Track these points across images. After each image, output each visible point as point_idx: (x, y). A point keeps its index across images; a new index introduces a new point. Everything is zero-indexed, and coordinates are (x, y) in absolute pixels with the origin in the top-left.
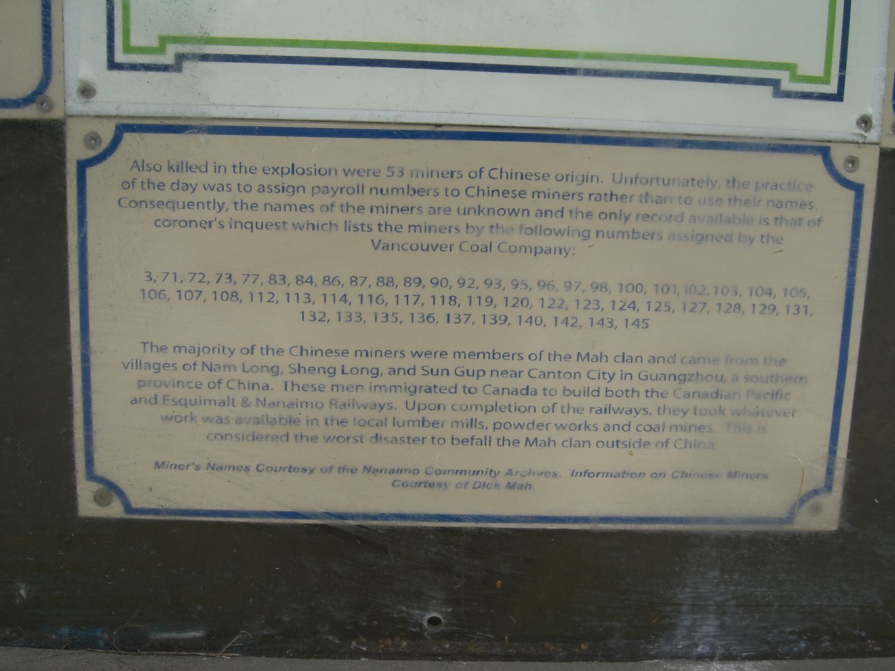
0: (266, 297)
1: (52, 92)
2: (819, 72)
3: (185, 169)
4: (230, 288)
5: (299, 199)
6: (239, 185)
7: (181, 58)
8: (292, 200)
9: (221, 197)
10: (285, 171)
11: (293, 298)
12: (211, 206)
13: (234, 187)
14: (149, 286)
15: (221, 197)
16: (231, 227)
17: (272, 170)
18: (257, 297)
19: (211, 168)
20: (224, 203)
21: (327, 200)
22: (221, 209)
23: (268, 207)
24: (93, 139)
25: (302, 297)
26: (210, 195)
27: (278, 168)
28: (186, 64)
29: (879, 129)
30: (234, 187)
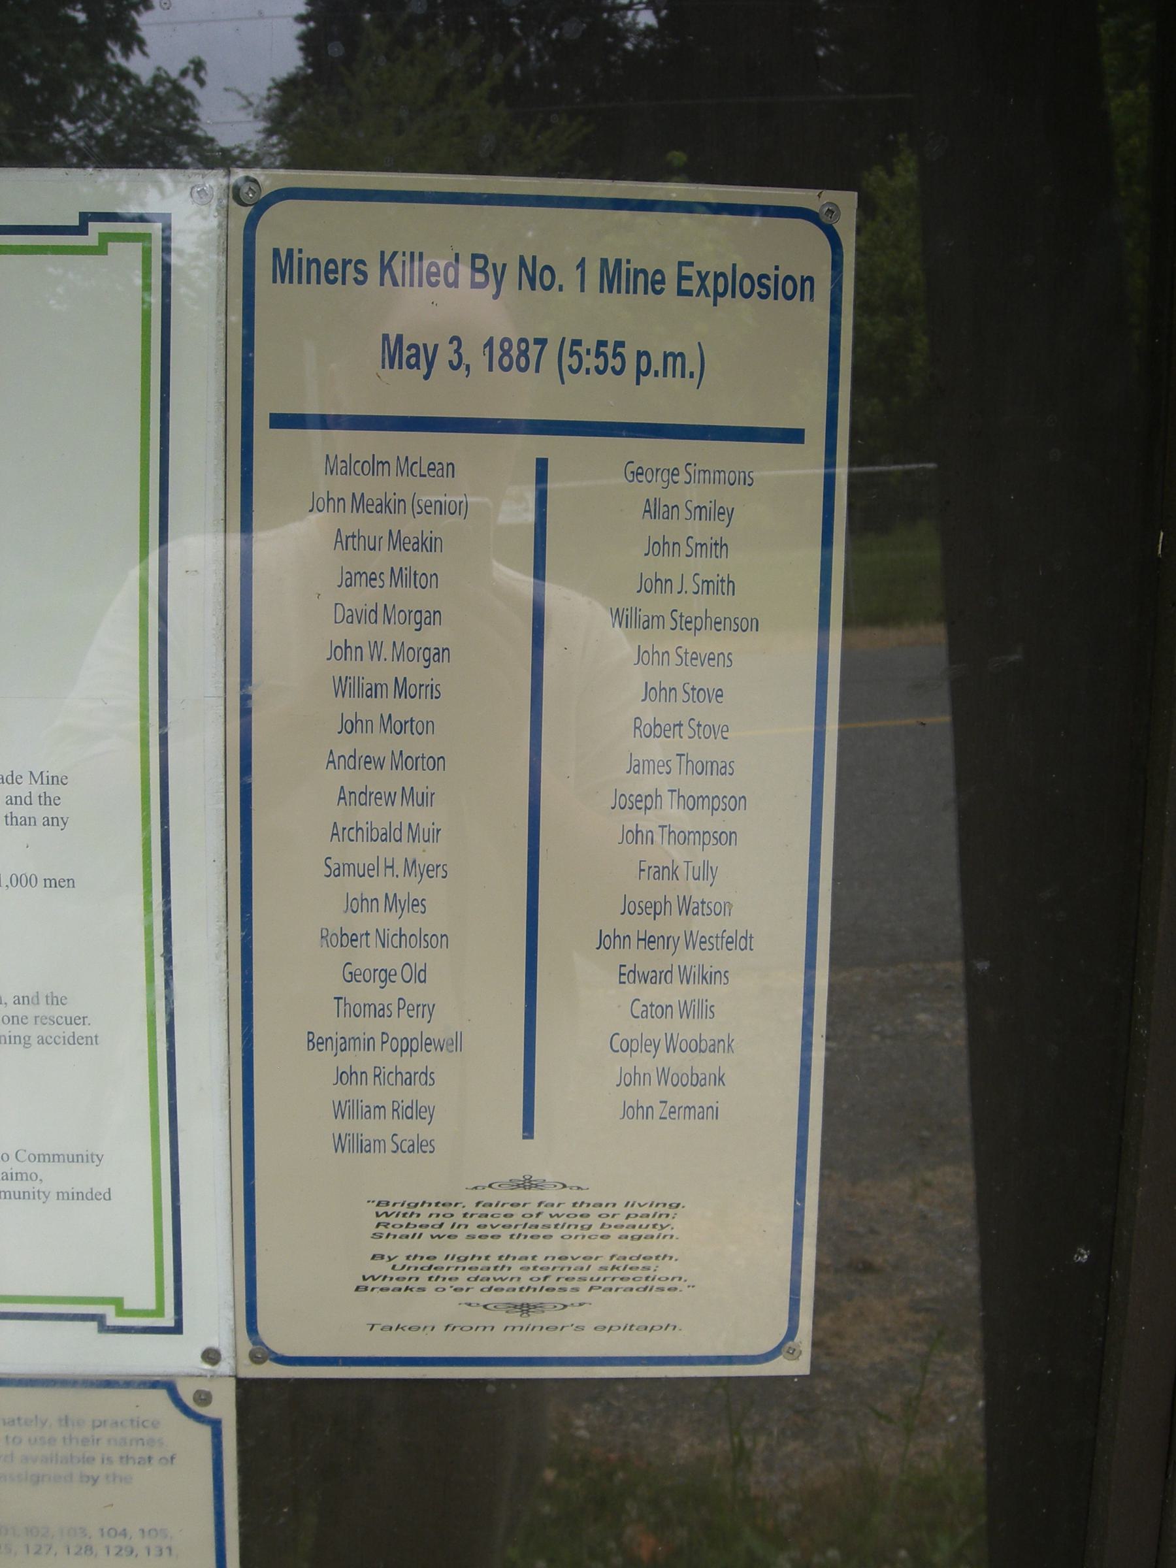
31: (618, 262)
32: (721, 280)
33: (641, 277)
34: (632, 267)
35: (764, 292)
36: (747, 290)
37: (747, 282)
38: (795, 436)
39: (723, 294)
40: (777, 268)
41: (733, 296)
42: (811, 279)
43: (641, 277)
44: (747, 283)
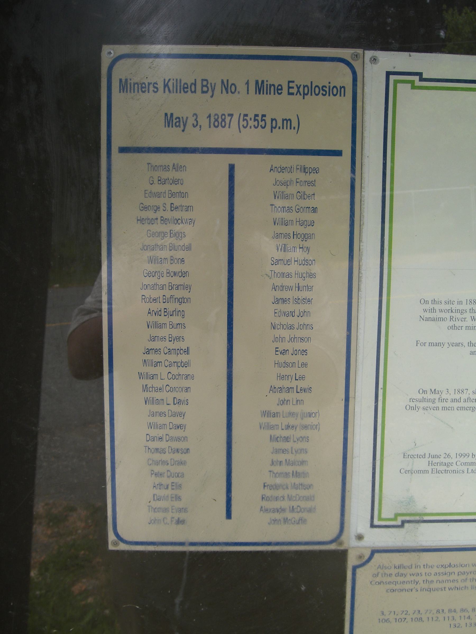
0: (435, 619)
1: (343, 538)
3: (402, 568)
4: (419, 616)
5: (452, 577)
6: (426, 573)
7: (403, 522)
8: (448, 578)
9: (417, 578)
10: (447, 566)
11: (447, 619)
12: (413, 582)
13: (424, 574)
14: (381, 617)
15: (417, 578)
16: (421, 591)
17: (441, 566)
18: (430, 619)
19: (414, 566)
20: (418, 581)
21: (464, 577)
22: (417, 584)
23: (438, 582)
24: (360, 557)
25: (451, 618)
26: (413, 578)
27: (443, 565)
28: (406, 525)
30: (424, 574)
31: (263, 82)
32: (306, 88)
33: (272, 87)
34: (269, 83)
35: (324, 93)
36: (317, 92)
37: (317, 89)
38: (338, 153)
39: (307, 94)
40: (329, 83)
41: (311, 95)
42: (344, 87)
43: (272, 87)
44: (317, 90)
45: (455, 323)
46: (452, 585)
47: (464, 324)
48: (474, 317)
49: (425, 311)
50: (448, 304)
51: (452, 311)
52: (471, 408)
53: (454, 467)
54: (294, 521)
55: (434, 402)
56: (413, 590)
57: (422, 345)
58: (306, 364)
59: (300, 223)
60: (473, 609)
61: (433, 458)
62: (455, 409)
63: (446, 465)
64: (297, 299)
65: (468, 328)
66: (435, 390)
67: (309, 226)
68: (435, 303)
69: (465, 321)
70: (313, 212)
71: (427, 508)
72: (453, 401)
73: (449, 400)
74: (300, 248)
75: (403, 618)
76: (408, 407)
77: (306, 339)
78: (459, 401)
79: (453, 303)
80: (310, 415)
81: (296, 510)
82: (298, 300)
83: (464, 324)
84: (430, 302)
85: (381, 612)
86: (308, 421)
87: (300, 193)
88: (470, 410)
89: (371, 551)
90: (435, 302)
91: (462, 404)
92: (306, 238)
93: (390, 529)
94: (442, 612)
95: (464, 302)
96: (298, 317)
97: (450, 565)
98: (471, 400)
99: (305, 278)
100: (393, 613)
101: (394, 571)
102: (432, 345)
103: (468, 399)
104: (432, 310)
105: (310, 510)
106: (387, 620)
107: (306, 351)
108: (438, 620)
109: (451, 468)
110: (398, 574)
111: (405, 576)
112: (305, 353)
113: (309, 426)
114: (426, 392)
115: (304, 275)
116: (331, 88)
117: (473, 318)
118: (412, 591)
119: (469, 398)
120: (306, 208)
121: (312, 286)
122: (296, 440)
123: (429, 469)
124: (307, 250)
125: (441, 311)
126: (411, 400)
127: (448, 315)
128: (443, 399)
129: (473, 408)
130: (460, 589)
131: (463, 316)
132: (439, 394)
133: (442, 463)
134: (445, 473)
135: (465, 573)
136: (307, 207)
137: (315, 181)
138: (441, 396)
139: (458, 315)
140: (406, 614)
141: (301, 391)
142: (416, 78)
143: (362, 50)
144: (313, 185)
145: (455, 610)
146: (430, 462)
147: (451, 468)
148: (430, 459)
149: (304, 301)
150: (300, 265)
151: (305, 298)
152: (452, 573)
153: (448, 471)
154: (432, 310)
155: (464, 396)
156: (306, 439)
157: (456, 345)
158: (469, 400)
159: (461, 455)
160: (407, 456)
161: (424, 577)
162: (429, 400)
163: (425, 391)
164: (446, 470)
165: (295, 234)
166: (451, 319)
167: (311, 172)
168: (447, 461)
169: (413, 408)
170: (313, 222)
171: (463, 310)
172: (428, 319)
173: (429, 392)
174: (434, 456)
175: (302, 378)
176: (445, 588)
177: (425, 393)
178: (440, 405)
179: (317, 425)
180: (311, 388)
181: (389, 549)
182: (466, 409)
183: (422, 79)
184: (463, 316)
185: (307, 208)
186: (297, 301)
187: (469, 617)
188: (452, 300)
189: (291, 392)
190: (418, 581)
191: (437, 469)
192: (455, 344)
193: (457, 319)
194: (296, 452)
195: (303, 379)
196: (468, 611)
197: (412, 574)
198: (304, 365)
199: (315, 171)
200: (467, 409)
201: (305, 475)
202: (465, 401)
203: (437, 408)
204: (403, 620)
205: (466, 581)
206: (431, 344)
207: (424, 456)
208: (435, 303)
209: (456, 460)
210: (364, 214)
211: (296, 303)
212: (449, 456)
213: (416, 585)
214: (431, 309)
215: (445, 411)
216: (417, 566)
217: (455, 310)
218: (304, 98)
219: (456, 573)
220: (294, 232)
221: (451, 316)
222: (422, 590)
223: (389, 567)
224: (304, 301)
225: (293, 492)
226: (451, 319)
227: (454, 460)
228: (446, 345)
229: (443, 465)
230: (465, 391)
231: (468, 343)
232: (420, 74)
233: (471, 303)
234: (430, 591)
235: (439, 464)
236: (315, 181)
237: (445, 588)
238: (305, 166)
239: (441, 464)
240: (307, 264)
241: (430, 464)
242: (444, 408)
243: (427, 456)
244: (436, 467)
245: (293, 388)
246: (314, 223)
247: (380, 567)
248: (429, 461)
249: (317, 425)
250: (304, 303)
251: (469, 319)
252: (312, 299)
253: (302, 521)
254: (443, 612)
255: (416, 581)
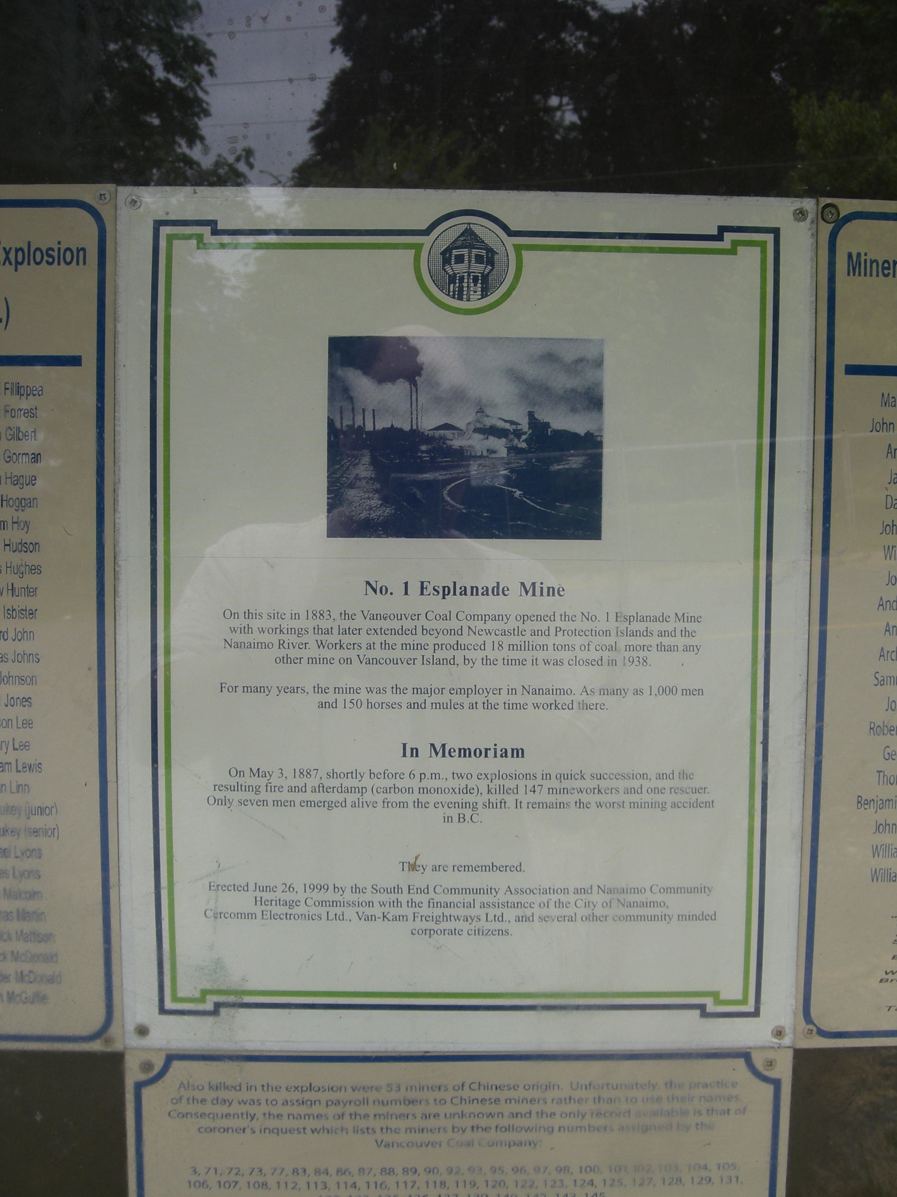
0: (290, 1186)
1: (114, 1030)
2: (740, 997)
3: (222, 1088)
4: (261, 1179)
5: (316, 1110)
6: (267, 1100)
7: (218, 1006)
8: (309, 1111)
9: (252, 1110)
10: (305, 1089)
11: (312, 1186)
12: (245, 1116)
13: (263, 1102)
14: (194, 1178)
15: (252, 1110)
16: (261, 1132)
17: (294, 1089)
18: (283, 1185)
19: (244, 1087)
20: (255, 1114)
21: (339, 1110)
22: (252, 1119)
23: (291, 1117)
24: (147, 1066)
25: (320, 1186)
26: (243, 1108)
27: (298, 1087)
28: (223, 1011)
29: (792, 1036)
30: (263, 1102)
32: (20, 253)
35: (50, 260)
36: (38, 259)
37: (38, 253)
38: (75, 361)
39: (21, 263)
40: (59, 243)
41: (29, 264)
42: (83, 249)
44: (38, 254)
45: (287, 651)
46: (318, 1124)
47: (305, 654)
48: (321, 641)
49: (233, 630)
50: (274, 618)
51: (281, 631)
52: (326, 803)
53: (301, 909)
54: (26, 998)
55: (257, 791)
56: (246, 1130)
57: (231, 690)
58: (30, 722)
59: (13, 480)
60: (338, 1171)
61: (263, 891)
62: (297, 804)
63: (286, 905)
64: (11, 609)
65: (312, 660)
66: (258, 769)
67: (27, 485)
68: (251, 617)
69: (305, 648)
70: (35, 461)
71: (247, 981)
72: (291, 790)
73: (286, 789)
74: (13, 523)
75: (233, 1182)
76: (212, 801)
77: (28, 679)
78: (303, 789)
79: (283, 617)
80: (42, 811)
81: (27, 979)
82: (13, 611)
83: (305, 654)
84: (242, 616)
85: (192, 1167)
86: (37, 822)
87: (12, 430)
88: (324, 806)
89: (164, 1057)
90: (251, 615)
91: (309, 796)
92: (23, 505)
93: (186, 1017)
94: (303, 1173)
95: (303, 616)
96: (14, 640)
97: (310, 1087)
98: (325, 788)
99: (22, 573)
100: (212, 1171)
101: (210, 1095)
102: (249, 691)
103: (319, 787)
104: (246, 629)
105: (52, 980)
106: (203, 1183)
107: (29, 700)
108: (298, 1187)
109: (296, 910)
110: (217, 1100)
111: (231, 1104)
112: (27, 703)
113: (41, 830)
114: (242, 773)
115: (22, 569)
116: (62, 252)
117: (319, 643)
118: (244, 1131)
119: (321, 785)
120: (23, 454)
121: (36, 588)
122: (19, 854)
123: (258, 910)
124: (26, 527)
125: (262, 631)
126: (217, 787)
127: (274, 638)
128: (275, 787)
129: (330, 803)
130: (333, 1132)
131: (304, 639)
132: (265, 776)
133: (280, 900)
134: (286, 918)
135: (339, 1103)
136: (24, 454)
137: (36, 409)
138: (269, 781)
139: (293, 639)
140: (236, 1174)
141: (25, 770)
142: (207, 230)
143: (115, 185)
144: (32, 416)
145: (327, 1170)
146: (259, 899)
147: (296, 910)
148: (258, 894)
149: (22, 614)
150: (14, 552)
151: (24, 609)
152: (315, 1101)
153: (292, 917)
154: (246, 629)
155: (313, 782)
156: (36, 853)
157: (292, 691)
158: (321, 789)
159: (313, 888)
160: (415, 890)
161: (264, 1108)
162: (248, 788)
163: (240, 772)
164: (289, 913)
165: (4, 498)
166: (281, 644)
167: (29, 393)
168: (288, 897)
169: (220, 801)
170: (33, 478)
171: (302, 629)
172: (238, 646)
173: (247, 773)
174: (265, 888)
175: (25, 746)
176: (304, 1129)
177: (240, 776)
178: (271, 797)
179: (54, 829)
180: (40, 764)
181: (187, 1053)
182: (316, 804)
183: (215, 232)
184: (304, 639)
185: (24, 456)
186: (11, 613)
187: (354, 1185)
188: (280, 612)
189: (7, 770)
190: (255, 1114)
191: (271, 911)
192: (290, 690)
193: (291, 644)
194: (22, 875)
195: (27, 748)
196: (352, 1174)
197: (243, 1101)
198: (28, 724)
199: (37, 392)
200: (286, 804)
201: (38, 916)
202: (314, 790)
203: (265, 803)
204: (233, 1185)
205: (343, 1118)
206: (247, 689)
207: (246, 888)
208: (251, 617)
209: (306, 895)
210: (120, 463)
211: (9, 616)
212: (291, 889)
213: (251, 1121)
214: (244, 627)
215: (420, 809)
216: (251, 1087)
217: (288, 629)
218: (16, 270)
219: (324, 1103)
220: (2, 496)
221: (280, 640)
222: (263, 1132)
223: (200, 1087)
224: (22, 614)
225: (20, 947)
226: (281, 646)
227: (301, 897)
228: (275, 691)
229: (281, 904)
230: (313, 773)
231: (314, 687)
232: (212, 223)
233: (316, 616)
234: (278, 1133)
235: (274, 903)
236: (36, 409)
237: (304, 1129)
238: (18, 384)
239: (278, 902)
240: (26, 550)
241: (258, 903)
242: (276, 803)
243: (252, 887)
244: (269, 908)
245: (10, 763)
246: (35, 480)
247: (184, 1086)
248: (256, 898)
249: (54, 829)
250: (22, 616)
251: (312, 645)
252: (36, 610)
253: (41, 998)
254: (305, 1174)
255: (250, 1115)
